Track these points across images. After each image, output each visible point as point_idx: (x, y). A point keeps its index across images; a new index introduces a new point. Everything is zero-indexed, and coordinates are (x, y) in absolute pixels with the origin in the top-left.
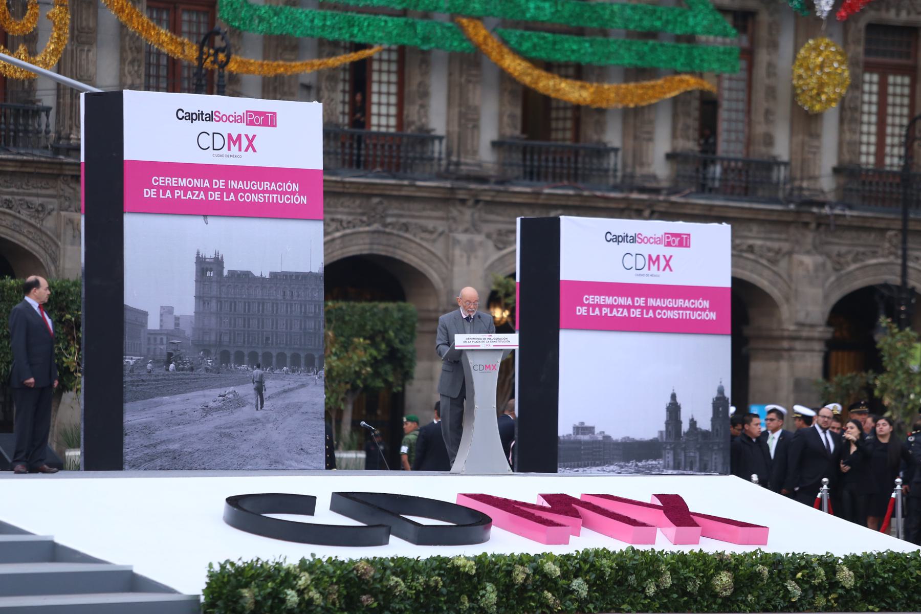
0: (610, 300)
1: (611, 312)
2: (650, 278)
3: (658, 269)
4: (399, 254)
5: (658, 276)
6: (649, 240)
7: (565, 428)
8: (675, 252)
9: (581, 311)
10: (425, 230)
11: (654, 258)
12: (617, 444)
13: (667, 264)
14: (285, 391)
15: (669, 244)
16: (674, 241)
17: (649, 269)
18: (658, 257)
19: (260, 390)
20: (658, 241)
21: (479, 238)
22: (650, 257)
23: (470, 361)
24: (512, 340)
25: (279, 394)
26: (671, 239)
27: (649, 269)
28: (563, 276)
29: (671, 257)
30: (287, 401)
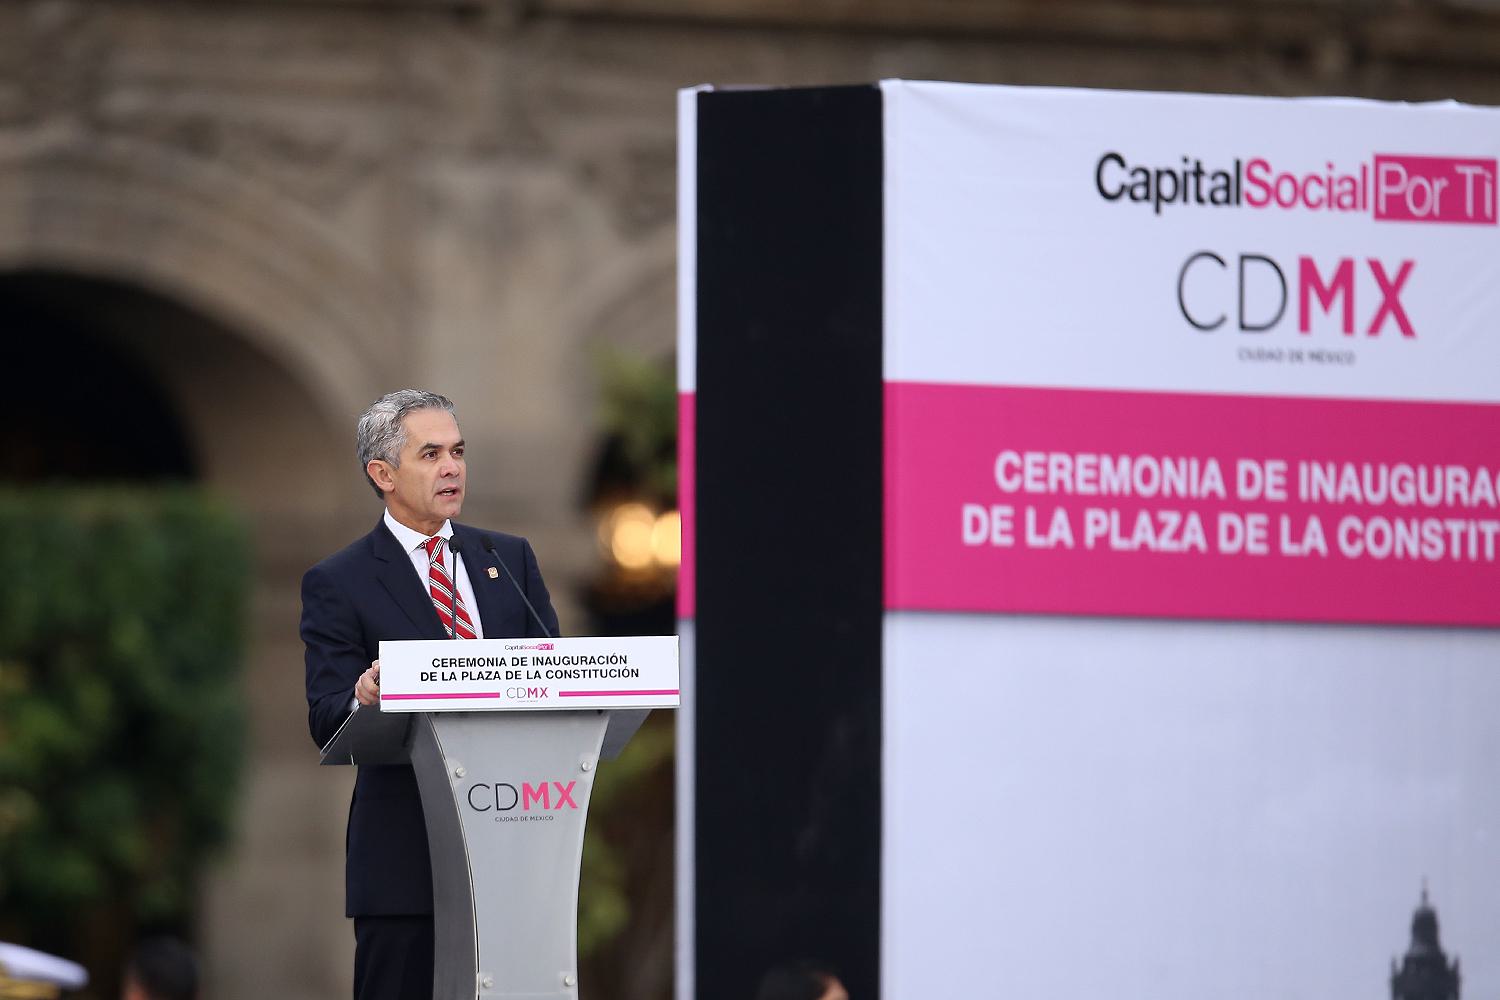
0: (1119, 475)
1: (1127, 530)
2: (1309, 367)
3: (1348, 327)
5: (1349, 358)
6: (1300, 192)
9: (985, 526)
10: (285, 147)
11: (1327, 275)
13: (1391, 303)
15: (1395, 210)
16: (1420, 196)
17: (1304, 325)
18: (1346, 271)
20: (1343, 195)
21: (541, 185)
22: (1308, 269)
23: (452, 766)
24: (658, 668)
26: (1406, 186)
27: (1304, 325)
28: (907, 357)
29: (1406, 268)
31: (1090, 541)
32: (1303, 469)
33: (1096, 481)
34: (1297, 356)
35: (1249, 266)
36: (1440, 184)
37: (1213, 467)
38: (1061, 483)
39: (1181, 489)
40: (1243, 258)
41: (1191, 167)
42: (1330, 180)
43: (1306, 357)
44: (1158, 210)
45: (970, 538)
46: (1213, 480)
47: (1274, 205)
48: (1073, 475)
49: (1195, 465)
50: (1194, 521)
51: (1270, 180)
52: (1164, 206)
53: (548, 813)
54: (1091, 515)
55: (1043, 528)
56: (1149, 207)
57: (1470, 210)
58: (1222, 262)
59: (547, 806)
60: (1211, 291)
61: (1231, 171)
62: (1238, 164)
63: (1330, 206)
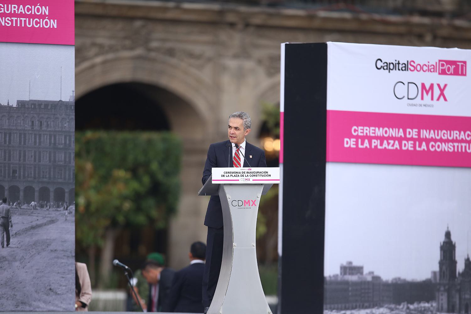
0: (380, 132)
1: (381, 145)
3: (432, 99)
4: (165, 81)
5: (432, 106)
6: (422, 68)
7: (331, 268)
8: (450, 80)
9: (349, 143)
10: (191, 55)
11: (428, 87)
12: (387, 285)
13: (442, 94)
14: (33, 228)
15: (443, 72)
17: (422, 98)
18: (432, 86)
19: (6, 226)
20: (431, 69)
21: (249, 64)
22: (423, 86)
23: (228, 196)
24: (275, 174)
25: (26, 230)
26: (446, 67)
27: (422, 98)
28: (331, 105)
29: (446, 86)
30: (35, 238)
31: (373, 147)
32: (422, 131)
33: (375, 133)
34: (421, 105)
35: (410, 84)
36: (453, 67)
37: (401, 130)
38: (367, 133)
39: (394, 135)
40: (409, 83)
41: (397, 62)
42: (429, 65)
43: (422, 105)
44: (389, 72)
45: (346, 146)
46: (401, 133)
47: (416, 71)
48: (369, 132)
49: (397, 130)
50: (397, 142)
51: (415, 65)
52: (391, 71)
53: (250, 207)
54: (373, 141)
55: (362, 144)
56: (388, 71)
57: (460, 73)
58: (404, 84)
59: (249, 205)
60: (401, 90)
61: (406, 63)
62: (408, 61)
63: (428, 71)
